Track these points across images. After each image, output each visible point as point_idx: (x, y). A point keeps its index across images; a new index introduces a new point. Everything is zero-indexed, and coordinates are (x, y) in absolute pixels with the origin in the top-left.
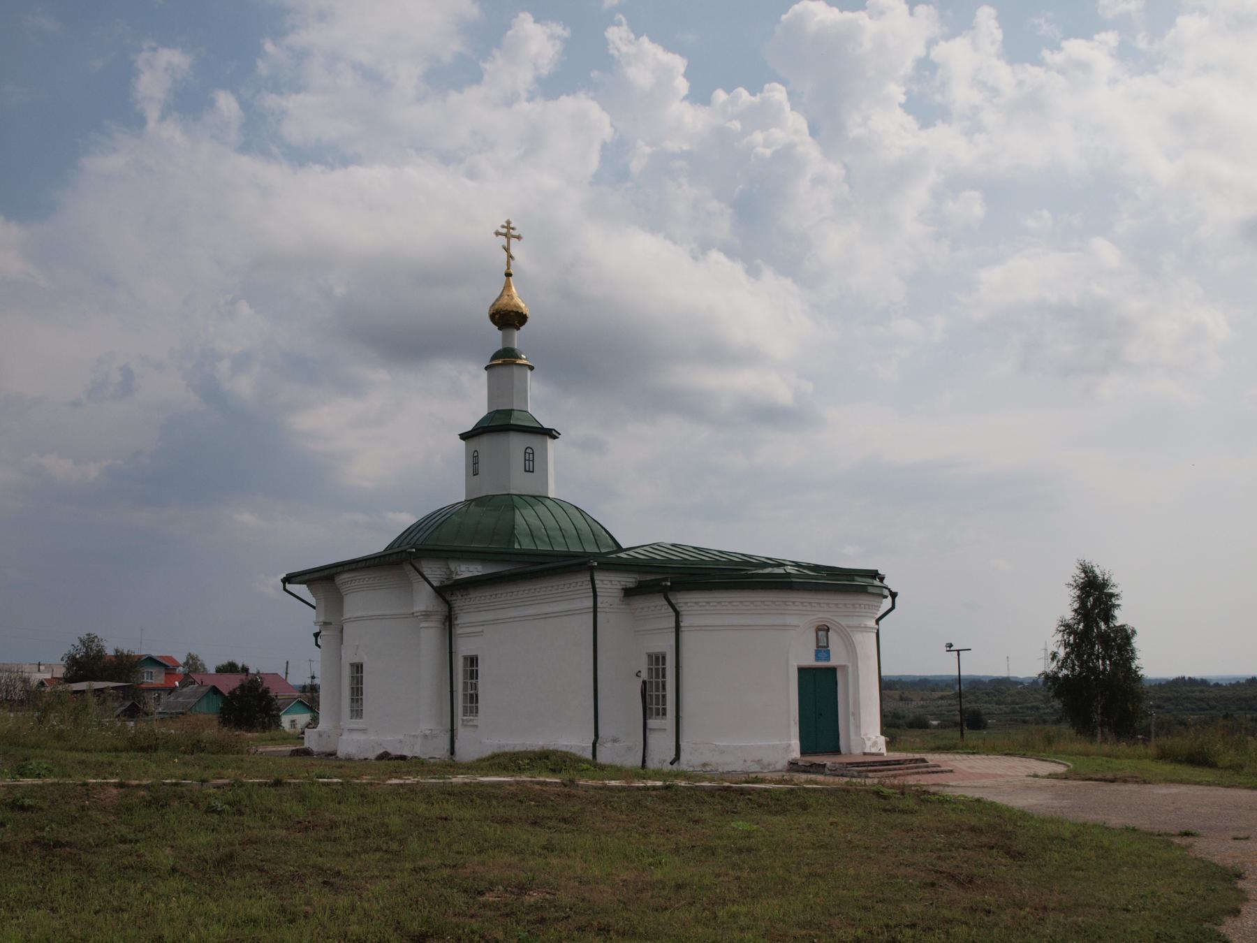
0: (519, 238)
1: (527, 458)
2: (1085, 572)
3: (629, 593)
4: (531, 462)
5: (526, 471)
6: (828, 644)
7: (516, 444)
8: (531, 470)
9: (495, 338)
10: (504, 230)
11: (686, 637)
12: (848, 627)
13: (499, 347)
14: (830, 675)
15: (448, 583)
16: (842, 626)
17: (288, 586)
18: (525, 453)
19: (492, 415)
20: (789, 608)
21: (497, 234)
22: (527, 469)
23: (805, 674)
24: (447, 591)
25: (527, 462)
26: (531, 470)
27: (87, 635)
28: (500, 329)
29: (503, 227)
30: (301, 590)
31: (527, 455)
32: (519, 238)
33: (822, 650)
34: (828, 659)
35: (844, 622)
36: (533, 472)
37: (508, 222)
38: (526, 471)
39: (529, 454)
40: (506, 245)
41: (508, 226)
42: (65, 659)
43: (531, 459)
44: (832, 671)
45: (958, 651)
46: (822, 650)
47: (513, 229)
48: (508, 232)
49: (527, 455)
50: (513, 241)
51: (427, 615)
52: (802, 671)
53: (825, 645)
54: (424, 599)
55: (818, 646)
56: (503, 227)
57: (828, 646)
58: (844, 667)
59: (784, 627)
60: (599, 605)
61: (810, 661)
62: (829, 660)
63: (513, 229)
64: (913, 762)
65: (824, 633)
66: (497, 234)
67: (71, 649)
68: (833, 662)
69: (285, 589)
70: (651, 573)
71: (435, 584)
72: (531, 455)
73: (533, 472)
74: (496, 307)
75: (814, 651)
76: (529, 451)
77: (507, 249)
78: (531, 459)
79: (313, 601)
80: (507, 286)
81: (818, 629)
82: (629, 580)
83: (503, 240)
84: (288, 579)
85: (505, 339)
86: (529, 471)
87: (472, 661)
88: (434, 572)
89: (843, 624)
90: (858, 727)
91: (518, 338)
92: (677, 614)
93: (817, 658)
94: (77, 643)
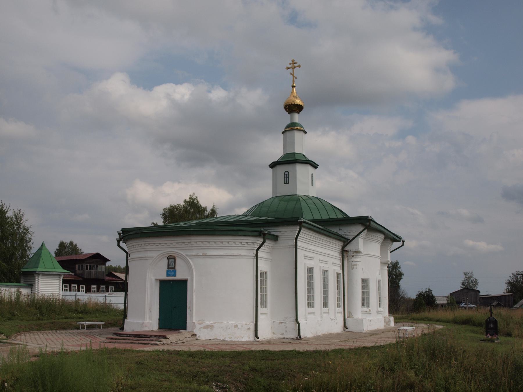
0: (299, 66)
1: (285, 177)
4: (287, 179)
5: (284, 183)
6: (175, 266)
7: (281, 170)
8: (287, 182)
9: (286, 118)
12: (187, 256)
13: (289, 122)
14: (184, 283)
16: (183, 255)
18: (284, 174)
20: (193, 246)
21: (288, 68)
22: (285, 182)
25: (285, 179)
26: (287, 182)
28: (289, 114)
31: (285, 175)
32: (299, 66)
33: (171, 269)
35: (183, 253)
36: (288, 183)
37: (293, 62)
38: (284, 183)
39: (286, 174)
40: (292, 73)
41: (293, 62)
43: (287, 177)
44: (184, 283)
46: (171, 269)
47: (296, 63)
48: (293, 66)
49: (285, 175)
52: (163, 284)
53: (174, 267)
55: (168, 268)
57: (174, 268)
59: (146, 258)
61: (164, 277)
62: (175, 276)
63: (296, 63)
64: (157, 337)
65: (173, 260)
66: (288, 68)
68: (179, 276)
72: (288, 175)
73: (288, 183)
75: (166, 271)
76: (287, 173)
77: (292, 74)
78: (287, 177)
81: (169, 258)
85: (292, 118)
86: (287, 183)
89: (184, 255)
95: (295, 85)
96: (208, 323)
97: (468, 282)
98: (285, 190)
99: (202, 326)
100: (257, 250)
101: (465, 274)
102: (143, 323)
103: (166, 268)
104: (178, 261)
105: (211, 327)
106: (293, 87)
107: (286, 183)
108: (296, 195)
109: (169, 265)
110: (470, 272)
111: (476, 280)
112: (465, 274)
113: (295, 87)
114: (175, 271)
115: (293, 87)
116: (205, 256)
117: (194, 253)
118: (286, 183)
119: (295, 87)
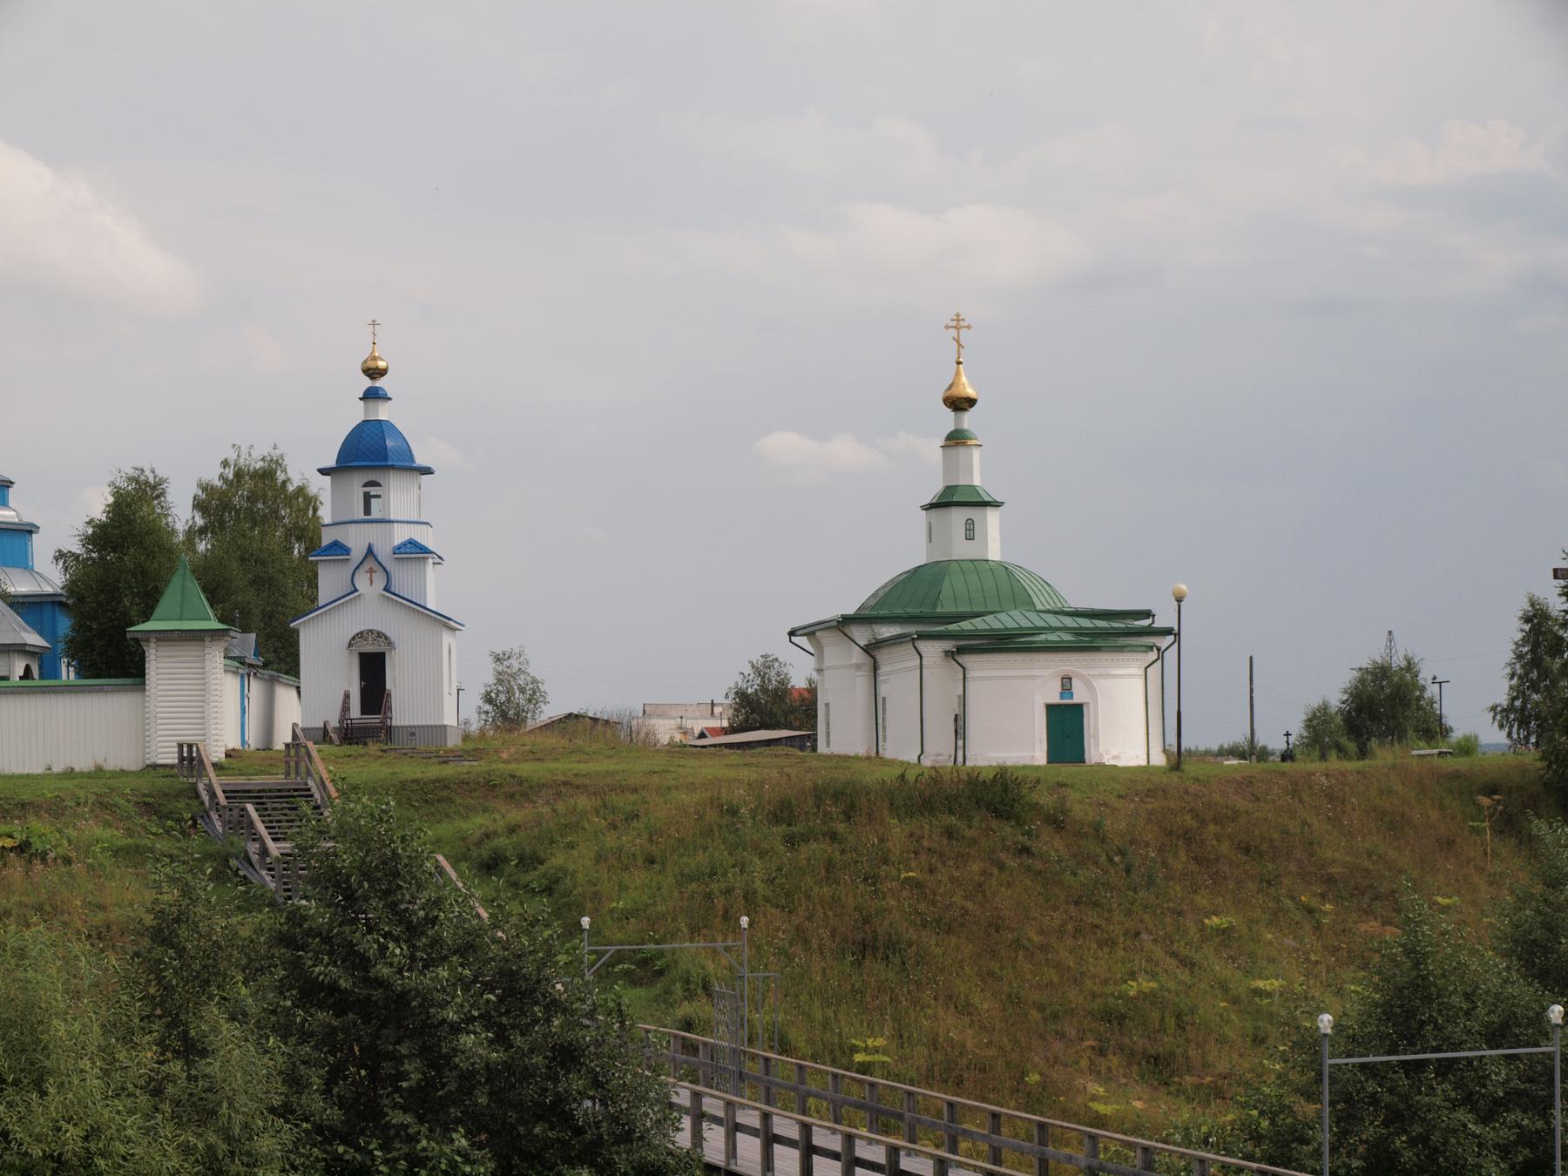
0: (969, 327)
2: (1532, 605)
3: (949, 654)
7: (958, 516)
10: (954, 323)
11: (971, 686)
13: (952, 428)
14: (1079, 708)
15: (874, 641)
17: (793, 639)
19: (949, 490)
21: (947, 327)
23: (1051, 709)
24: (871, 649)
27: (762, 656)
29: (952, 320)
30: (803, 641)
32: (969, 327)
34: (1071, 697)
35: (1084, 672)
37: (958, 315)
41: (958, 318)
42: (732, 696)
44: (1079, 708)
45: (1440, 683)
47: (963, 320)
48: (958, 323)
50: (963, 331)
51: (858, 667)
52: (1051, 709)
54: (857, 656)
56: (952, 320)
58: (1088, 703)
59: (1032, 677)
60: (924, 663)
61: (1055, 699)
63: (963, 320)
66: (947, 327)
67: (739, 679)
68: (1076, 700)
69: (791, 641)
70: (975, 639)
71: (862, 644)
74: (949, 392)
79: (812, 651)
80: (958, 368)
82: (949, 645)
83: (953, 332)
84: (792, 633)
85: (957, 421)
87: (884, 699)
88: (862, 635)
90: (1097, 745)
91: (969, 420)
92: (964, 668)
93: (1062, 697)
94: (748, 670)
95: (961, 360)
96: (1116, 753)
97: (509, 691)
98: (962, 550)
99: (1110, 757)
100: (1146, 668)
101: (498, 659)
102: (1033, 757)
103: (1059, 689)
104: (1074, 681)
105: (1115, 757)
106: (959, 363)
107: (970, 538)
108: (987, 561)
109: (1063, 685)
110: (516, 650)
111: (535, 681)
112: (498, 659)
113: (961, 363)
114: (1072, 693)
115: (959, 363)
116: (1109, 676)
117: (1096, 672)
118: (970, 538)
119: (961, 363)
